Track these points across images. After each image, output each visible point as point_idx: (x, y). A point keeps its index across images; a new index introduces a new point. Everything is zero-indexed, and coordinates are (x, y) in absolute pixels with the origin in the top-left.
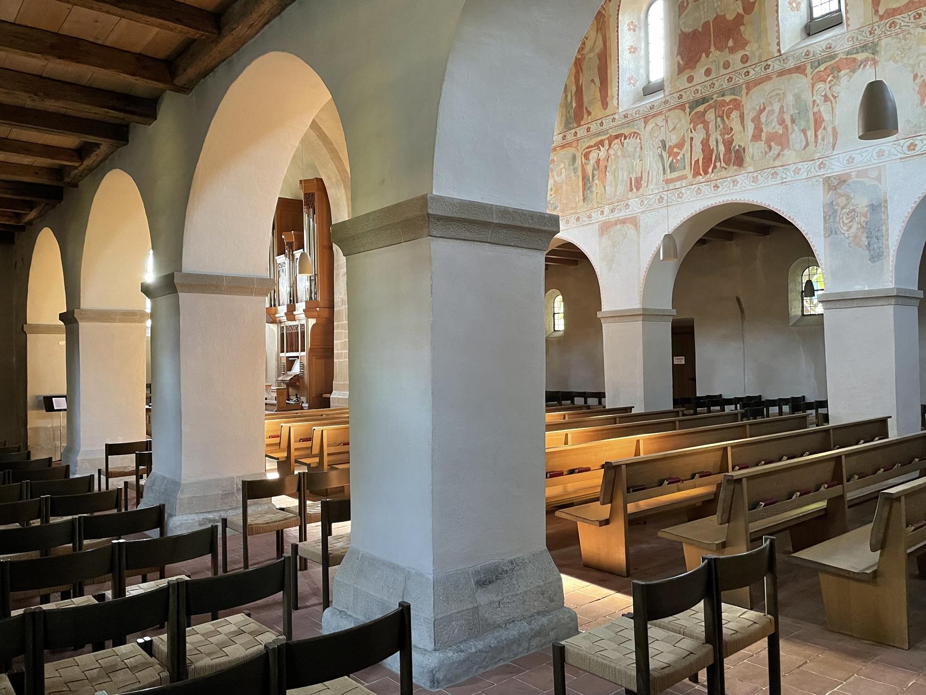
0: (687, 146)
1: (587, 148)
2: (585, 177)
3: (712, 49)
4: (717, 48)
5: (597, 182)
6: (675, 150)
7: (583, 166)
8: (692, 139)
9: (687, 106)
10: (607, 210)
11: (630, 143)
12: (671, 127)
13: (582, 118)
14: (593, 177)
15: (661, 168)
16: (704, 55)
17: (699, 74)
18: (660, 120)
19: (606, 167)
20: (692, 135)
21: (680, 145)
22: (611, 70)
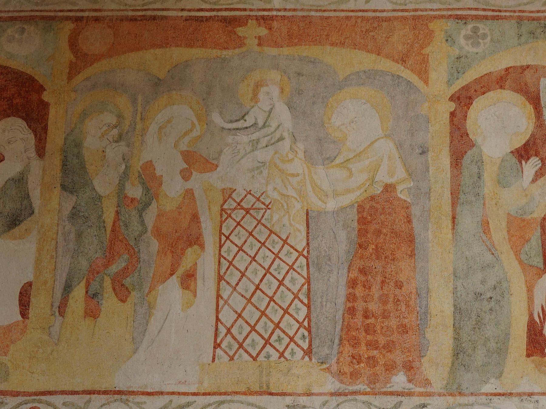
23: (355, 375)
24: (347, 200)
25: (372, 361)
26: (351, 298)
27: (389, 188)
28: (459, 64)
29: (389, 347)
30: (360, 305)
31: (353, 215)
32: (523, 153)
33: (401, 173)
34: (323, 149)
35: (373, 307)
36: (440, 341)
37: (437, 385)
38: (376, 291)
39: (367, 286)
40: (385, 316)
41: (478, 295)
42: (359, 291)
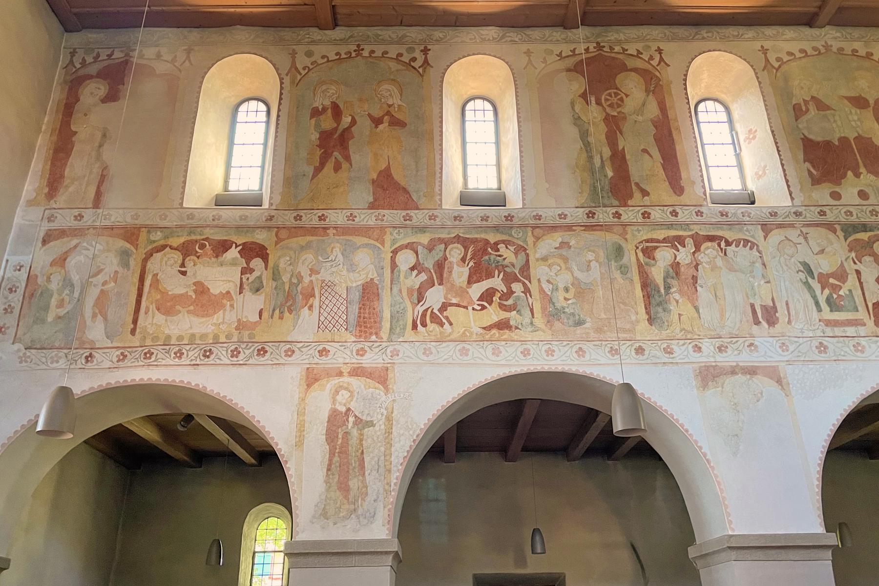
0: (852, 279)
1: (647, 241)
2: (647, 284)
3: (862, 170)
4: (869, 172)
5: (677, 296)
6: (831, 280)
7: (640, 266)
8: (858, 272)
9: (838, 227)
10: (708, 346)
11: (740, 255)
12: (817, 249)
13: (631, 196)
14: (668, 288)
15: (811, 302)
16: (850, 173)
17: (849, 191)
18: (793, 234)
19: (695, 279)
20: (856, 267)
21: (841, 275)
22: (682, 148)
23: (360, 336)
24: (359, 283)
25: (366, 332)
26: (360, 313)
27: (372, 279)
28: (394, 241)
29: (371, 328)
30: (362, 315)
31: (361, 287)
32: (412, 269)
33: (375, 275)
34: (352, 268)
35: (366, 315)
36: (386, 325)
37: (385, 339)
38: (367, 311)
39: (364, 309)
40: (370, 318)
41: (398, 312)
42: (362, 311)
